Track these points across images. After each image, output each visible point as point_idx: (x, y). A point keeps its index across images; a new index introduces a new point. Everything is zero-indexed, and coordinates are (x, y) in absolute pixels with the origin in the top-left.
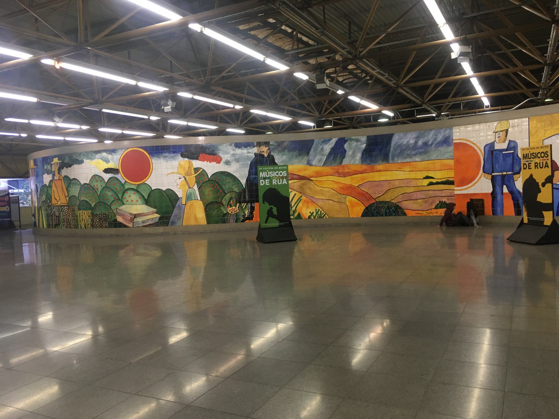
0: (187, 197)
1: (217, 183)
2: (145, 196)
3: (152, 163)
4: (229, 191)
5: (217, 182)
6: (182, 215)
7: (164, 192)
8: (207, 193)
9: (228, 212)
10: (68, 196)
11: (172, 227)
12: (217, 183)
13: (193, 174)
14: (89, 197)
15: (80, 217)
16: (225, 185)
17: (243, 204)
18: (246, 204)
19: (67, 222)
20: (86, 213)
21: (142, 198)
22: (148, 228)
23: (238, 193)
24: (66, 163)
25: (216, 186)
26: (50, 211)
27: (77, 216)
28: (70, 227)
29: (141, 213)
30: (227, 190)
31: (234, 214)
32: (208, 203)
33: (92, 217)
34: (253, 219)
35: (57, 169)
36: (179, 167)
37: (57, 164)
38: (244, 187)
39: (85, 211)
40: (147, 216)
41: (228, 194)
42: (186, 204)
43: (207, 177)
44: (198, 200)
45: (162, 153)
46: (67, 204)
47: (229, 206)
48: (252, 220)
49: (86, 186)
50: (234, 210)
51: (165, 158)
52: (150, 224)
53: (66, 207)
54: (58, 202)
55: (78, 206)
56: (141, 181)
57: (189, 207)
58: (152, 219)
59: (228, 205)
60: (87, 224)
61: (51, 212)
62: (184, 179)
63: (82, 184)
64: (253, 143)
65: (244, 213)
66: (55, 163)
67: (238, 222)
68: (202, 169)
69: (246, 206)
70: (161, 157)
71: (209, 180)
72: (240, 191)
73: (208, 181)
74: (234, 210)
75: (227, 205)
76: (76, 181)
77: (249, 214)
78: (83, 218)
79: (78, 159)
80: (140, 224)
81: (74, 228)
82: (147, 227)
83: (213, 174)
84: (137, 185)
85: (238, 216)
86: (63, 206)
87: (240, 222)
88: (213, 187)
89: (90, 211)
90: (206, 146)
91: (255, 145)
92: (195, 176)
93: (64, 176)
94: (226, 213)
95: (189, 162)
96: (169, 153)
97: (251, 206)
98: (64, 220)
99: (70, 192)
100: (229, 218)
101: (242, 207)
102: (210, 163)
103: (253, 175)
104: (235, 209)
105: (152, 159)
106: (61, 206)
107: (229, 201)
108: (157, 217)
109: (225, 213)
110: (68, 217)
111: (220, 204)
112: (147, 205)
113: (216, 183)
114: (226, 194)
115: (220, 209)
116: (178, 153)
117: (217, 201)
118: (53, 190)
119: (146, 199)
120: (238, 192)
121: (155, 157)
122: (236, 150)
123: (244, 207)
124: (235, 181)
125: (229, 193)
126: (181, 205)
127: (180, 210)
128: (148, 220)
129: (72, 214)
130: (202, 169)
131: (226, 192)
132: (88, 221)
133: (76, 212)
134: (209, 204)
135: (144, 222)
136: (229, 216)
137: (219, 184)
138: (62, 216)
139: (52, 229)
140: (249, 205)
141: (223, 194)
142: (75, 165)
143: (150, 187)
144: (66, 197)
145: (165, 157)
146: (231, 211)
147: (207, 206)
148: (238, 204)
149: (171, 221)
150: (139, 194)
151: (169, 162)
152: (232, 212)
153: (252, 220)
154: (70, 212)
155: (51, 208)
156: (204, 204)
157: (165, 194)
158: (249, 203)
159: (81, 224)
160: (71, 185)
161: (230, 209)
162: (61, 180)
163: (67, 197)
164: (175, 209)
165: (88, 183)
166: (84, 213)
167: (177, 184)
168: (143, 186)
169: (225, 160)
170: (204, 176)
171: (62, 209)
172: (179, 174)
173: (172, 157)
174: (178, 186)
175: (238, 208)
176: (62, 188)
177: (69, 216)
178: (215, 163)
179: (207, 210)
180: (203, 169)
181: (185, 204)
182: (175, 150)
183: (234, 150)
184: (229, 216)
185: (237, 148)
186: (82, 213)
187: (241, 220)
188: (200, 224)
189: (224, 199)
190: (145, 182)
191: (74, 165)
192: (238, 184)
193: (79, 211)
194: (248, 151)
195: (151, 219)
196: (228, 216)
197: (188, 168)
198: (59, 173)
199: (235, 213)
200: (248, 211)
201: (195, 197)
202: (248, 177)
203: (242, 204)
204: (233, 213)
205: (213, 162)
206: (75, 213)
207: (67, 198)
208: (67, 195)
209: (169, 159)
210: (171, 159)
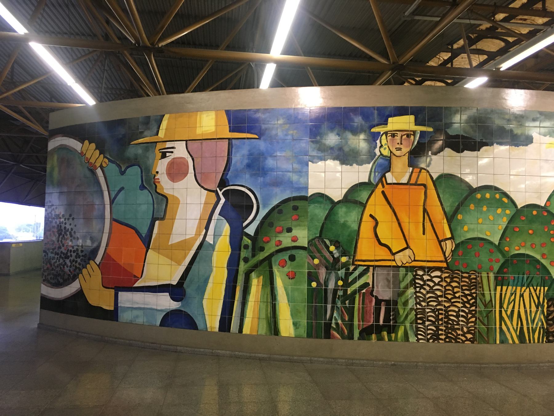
10: (452, 238)
14: (543, 245)
15: (501, 306)
19: (438, 319)
20: (526, 295)
24: (457, 136)
26: (340, 283)
27: (489, 304)
28: (452, 339)
33: (548, 307)
35: (406, 150)
37: (408, 136)
39: (524, 288)
46: (444, 265)
49: (535, 213)
53: (438, 273)
54: (394, 254)
55: (498, 272)
60: (528, 328)
61: (347, 284)
63: (519, 207)
66: (399, 134)
76: (497, 196)
78: (512, 312)
79: (511, 131)
81: (472, 341)
86: (422, 268)
89: (542, 291)
93: (441, 177)
98: (423, 311)
99: (466, 228)
106: (412, 269)
110: (447, 305)
118: (371, 216)
129: (466, 296)
132: (533, 321)
133: (487, 292)
138: (411, 303)
139: (348, 341)
142: (495, 144)
144: (440, 242)
154: (456, 290)
155: (348, 274)
159: (504, 327)
160: (472, 206)
162: (425, 186)
163: (449, 243)
165: (543, 205)
166: (522, 296)
171: (414, 279)
176: (425, 211)
177: (449, 300)
186: (514, 293)
191: (492, 144)
193: (499, 288)
198: (412, 164)
206: (483, 295)
207: (449, 246)
208: (449, 235)
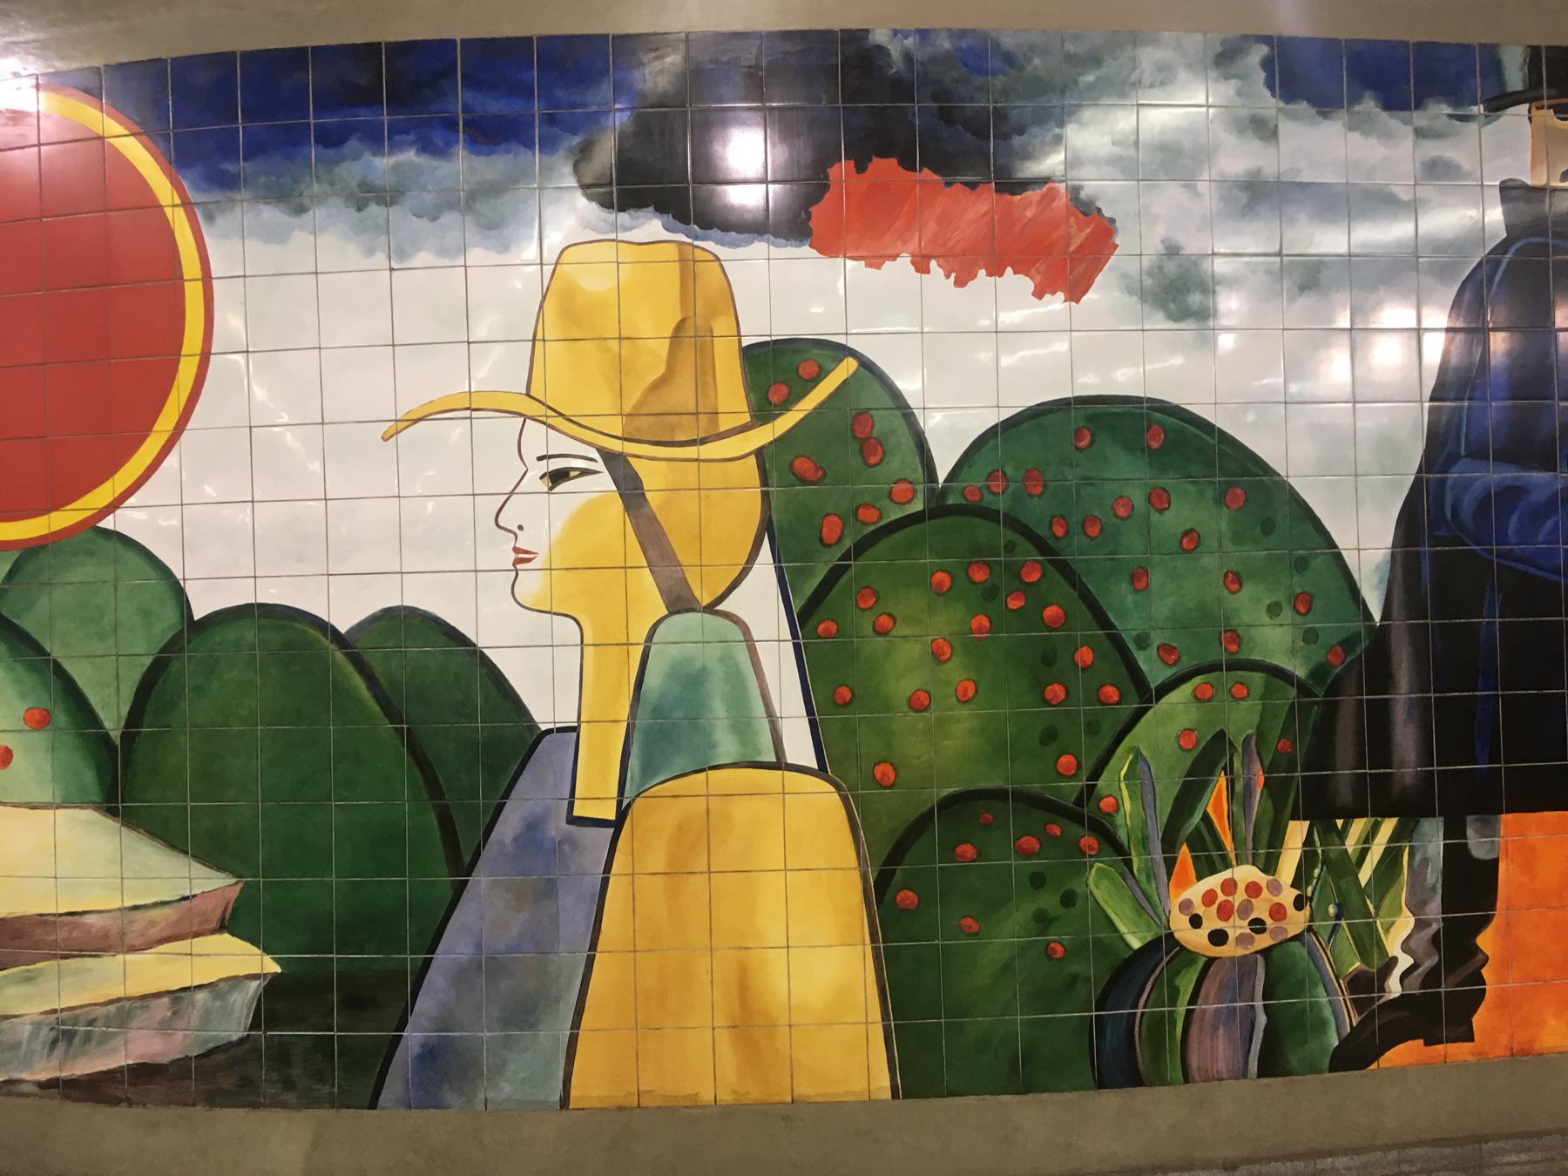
0: (642, 722)
1: (1042, 546)
2: (95, 700)
3: (207, 278)
4: (1187, 663)
5: (1042, 531)
6: (570, 959)
7: (339, 656)
8: (904, 686)
9: (1170, 936)
11: (419, 1116)
12: (1042, 546)
13: (725, 424)
16: (1138, 577)
17: (1358, 826)
18: (1388, 826)
21: (61, 718)
22: (122, 1110)
23: (1303, 688)
25: (1027, 589)
29: (43, 920)
30: (1165, 649)
31: (1244, 966)
32: (912, 815)
34: (1479, 1019)
36: (552, 329)
38: (1377, 615)
40: (111, 964)
41: (1175, 697)
42: (622, 813)
43: (919, 474)
44: (780, 764)
45: (332, 139)
47: (1184, 852)
48: (1469, 1037)
50: (1245, 909)
51: (374, 209)
52: (144, 1073)
56: (56, 507)
57: (658, 861)
58: (179, 996)
59: (1169, 845)
62: (604, 482)
64: (1494, 66)
65: (1368, 942)
67: (1294, 1058)
68: (849, 366)
69: (1391, 859)
70: (321, 199)
71: (939, 507)
72: (1319, 655)
73: (928, 525)
74: (1245, 909)
75: (1157, 847)
77: (1428, 964)
80: (27, 1063)
82: (115, 1102)
83: (991, 433)
84: (14, 555)
85: (1299, 989)
87: (1315, 1070)
88: (990, 594)
90: (908, 57)
91: (1515, 79)
92: (759, 453)
94: (1151, 948)
95: (688, 266)
96: (426, 147)
97: (1456, 856)
100: (1181, 1009)
101: (1344, 868)
102: (960, 283)
103: (1478, 453)
104: (1253, 889)
105: (210, 218)
107: (1190, 794)
108: (235, 981)
109: (1136, 944)
111: (1073, 829)
112: (112, 812)
113: (1023, 544)
114: (1147, 695)
115: (1068, 899)
116: (549, 145)
117: (1036, 787)
119: (105, 738)
120: (1301, 673)
121: (245, 194)
122: (1286, 128)
123: (1365, 875)
124: (1268, 527)
125: (1186, 690)
126: (558, 826)
127: (549, 890)
128: (125, 1010)
130: (849, 366)
131: (1154, 671)
134: (924, 821)
135: (69, 1036)
136: (1186, 983)
137: (1067, 572)
140: (1433, 839)
141: (1111, 692)
143: (155, 582)
145: (367, 196)
146: (1212, 923)
147: (897, 854)
148: (1297, 831)
149: (414, 1037)
150: (32, 668)
151: (423, 258)
152: (1218, 937)
153: (1469, 1037)
156: (859, 821)
157: (358, 681)
158: (1430, 814)
161: (1195, 891)
164: (481, 881)
167: (522, 557)
168: (85, 571)
169: (1153, 245)
170: (869, 447)
172: (554, 417)
173: (448, 202)
174: (532, 583)
175: (1295, 884)
178: (1026, 284)
179: (907, 897)
180: (866, 365)
181: (612, 816)
182: (495, 106)
183: (1264, 130)
184: (1186, 983)
185: (1303, 106)
187: (1336, 1043)
188: (806, 1089)
189: (1121, 764)
190: (107, 523)
192: (1301, 565)
194: (1433, 149)
195: (162, 1008)
196: (1174, 994)
197: (663, 348)
199: (1263, 941)
200: (1420, 925)
201: (742, 728)
202: (1417, 484)
203: (1342, 835)
204: (1228, 950)
205: (996, 271)
209: (421, 224)
210: (449, 218)
